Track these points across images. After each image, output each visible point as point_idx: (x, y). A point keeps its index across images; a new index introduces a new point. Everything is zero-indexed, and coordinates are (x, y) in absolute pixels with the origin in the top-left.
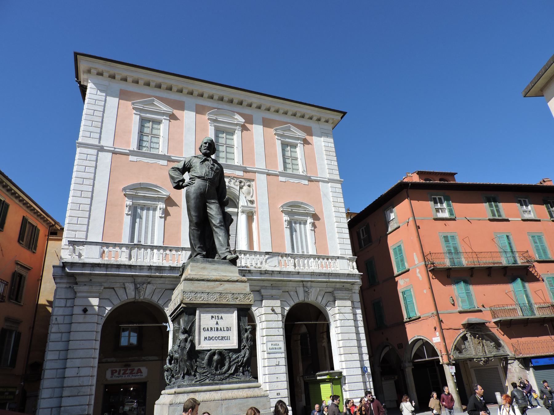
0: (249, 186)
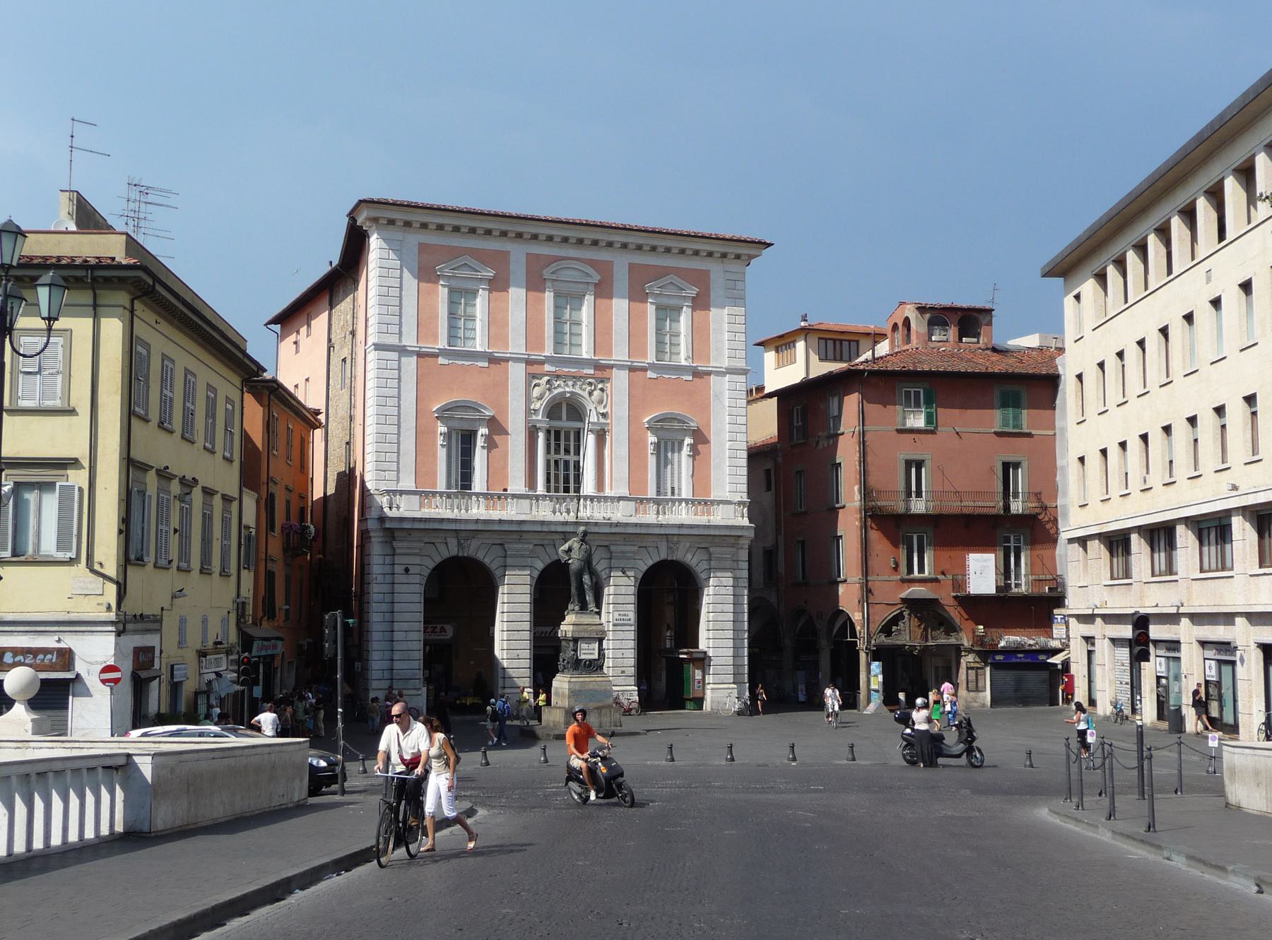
0: (602, 390)
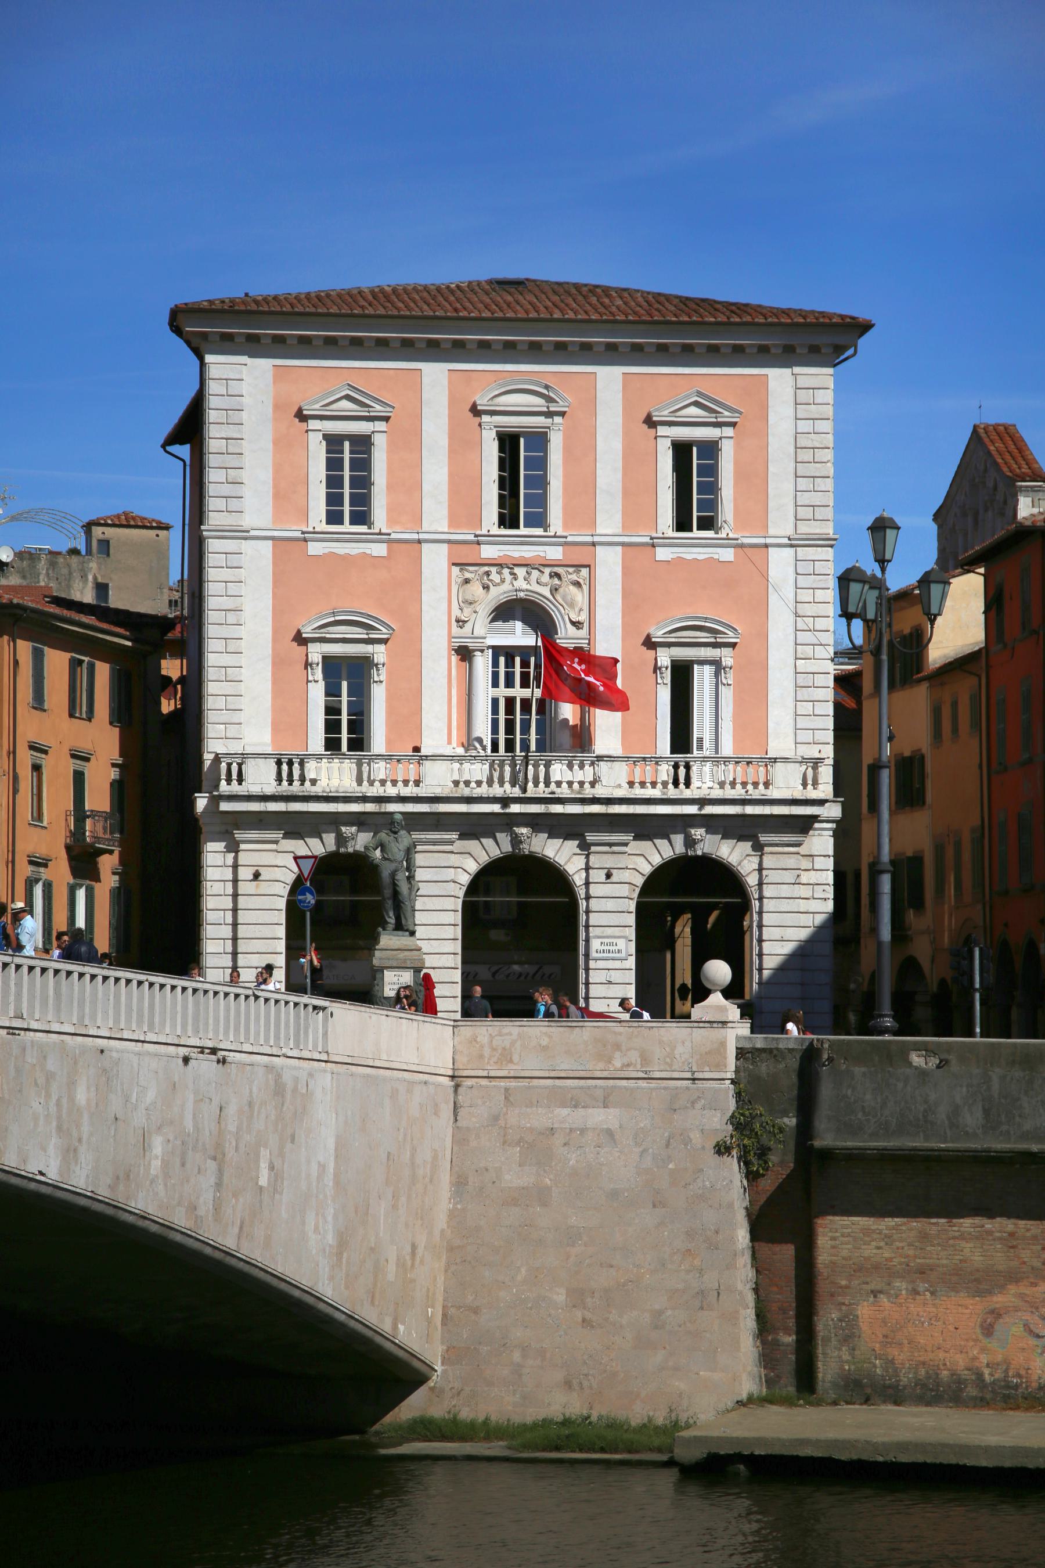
0: (577, 584)
